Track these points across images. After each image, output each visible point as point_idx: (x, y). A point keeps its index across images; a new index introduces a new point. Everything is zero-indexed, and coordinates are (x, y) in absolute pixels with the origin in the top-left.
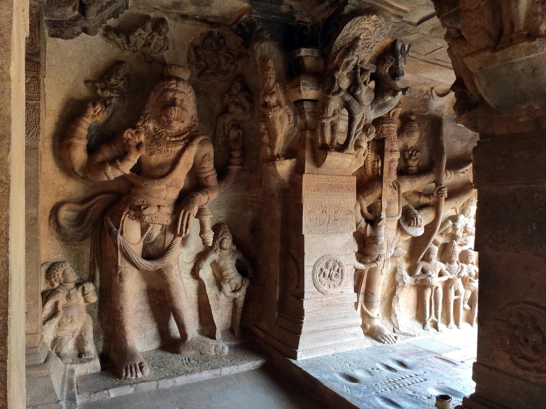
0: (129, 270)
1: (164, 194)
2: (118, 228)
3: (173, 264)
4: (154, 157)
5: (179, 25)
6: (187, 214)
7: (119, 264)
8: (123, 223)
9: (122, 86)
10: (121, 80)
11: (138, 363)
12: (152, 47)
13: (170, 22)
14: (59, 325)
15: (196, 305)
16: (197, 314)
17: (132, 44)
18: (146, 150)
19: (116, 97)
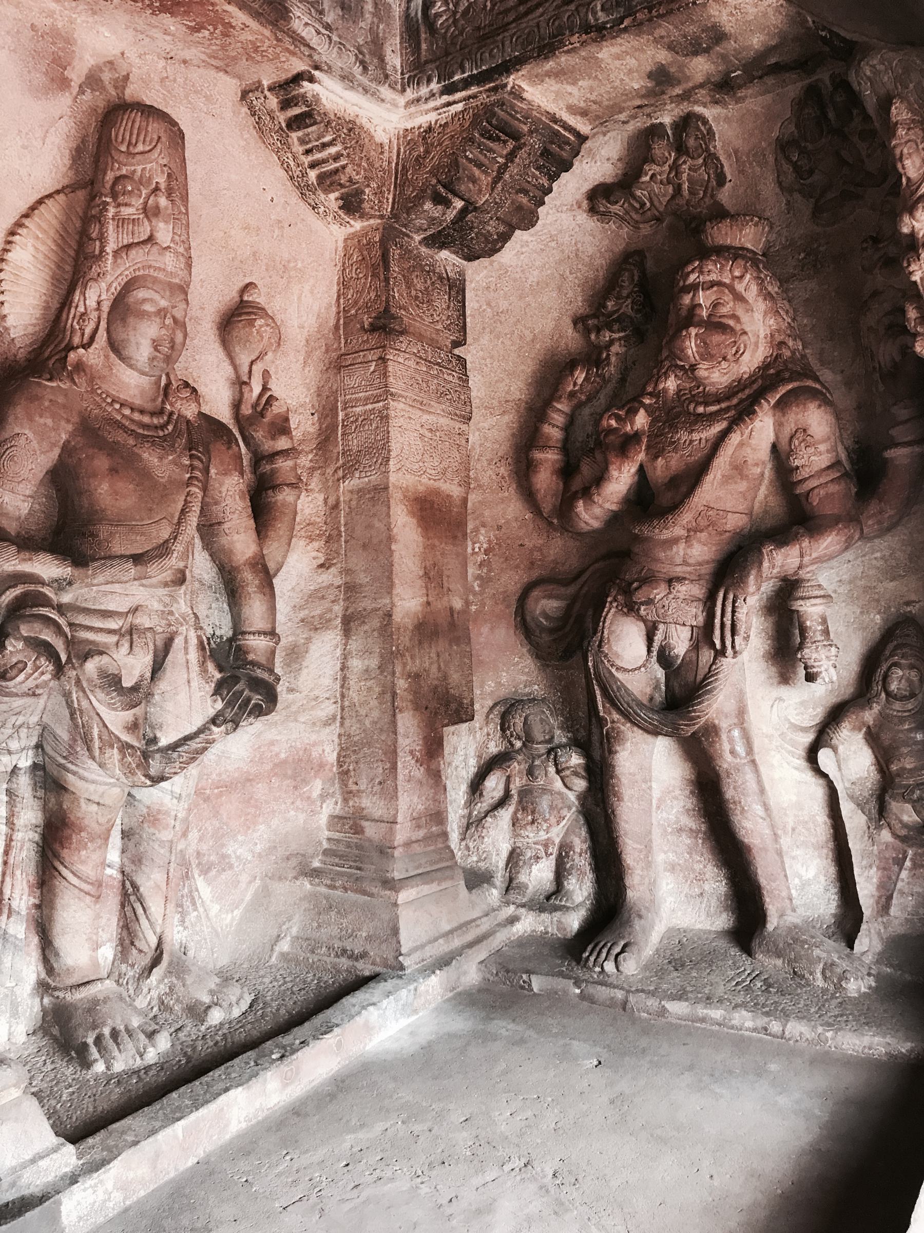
0: (622, 728)
1: (680, 550)
2: (595, 633)
3: (724, 724)
4: (660, 462)
5: (732, 109)
6: (731, 596)
7: (601, 714)
8: (604, 622)
9: (629, 311)
10: (628, 297)
11: (622, 943)
12: (686, 193)
13: (709, 113)
14: (514, 825)
15: (831, 845)
16: (832, 870)
17: (648, 204)
18: (648, 448)
19: (620, 339)
